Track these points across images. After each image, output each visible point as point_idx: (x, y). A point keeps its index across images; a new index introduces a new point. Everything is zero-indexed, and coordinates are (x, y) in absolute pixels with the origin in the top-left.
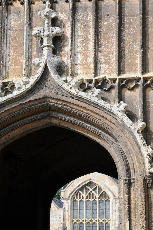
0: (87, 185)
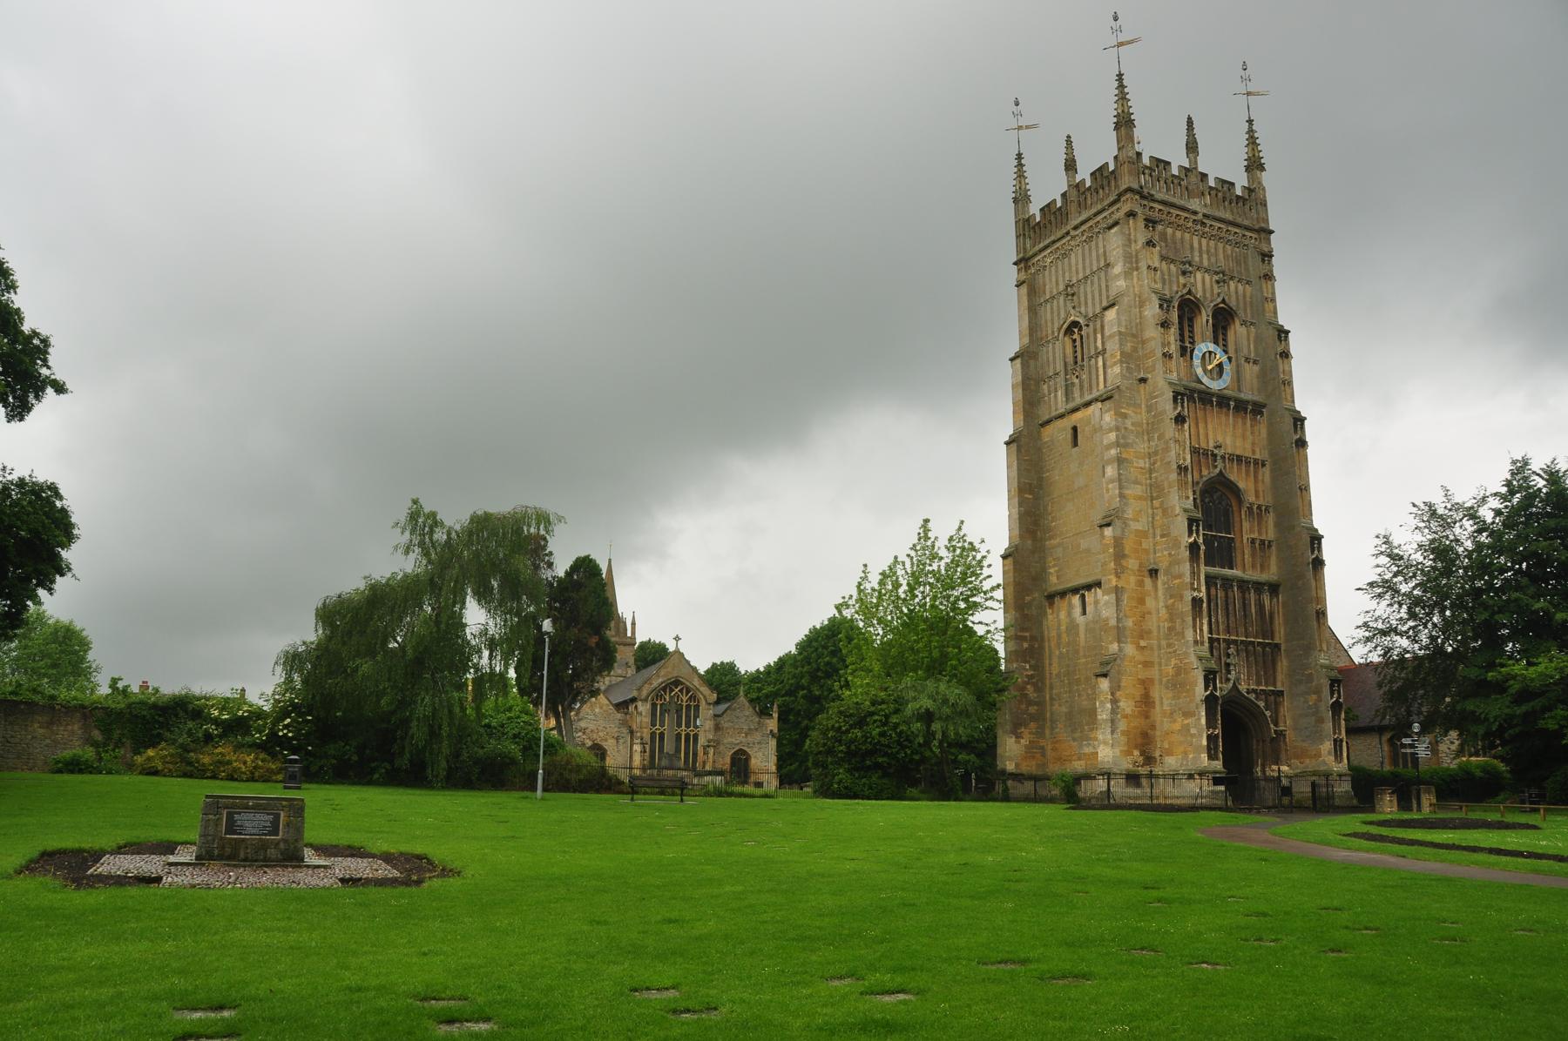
0: (670, 683)
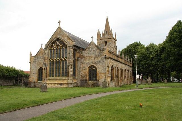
0: (56, 40)
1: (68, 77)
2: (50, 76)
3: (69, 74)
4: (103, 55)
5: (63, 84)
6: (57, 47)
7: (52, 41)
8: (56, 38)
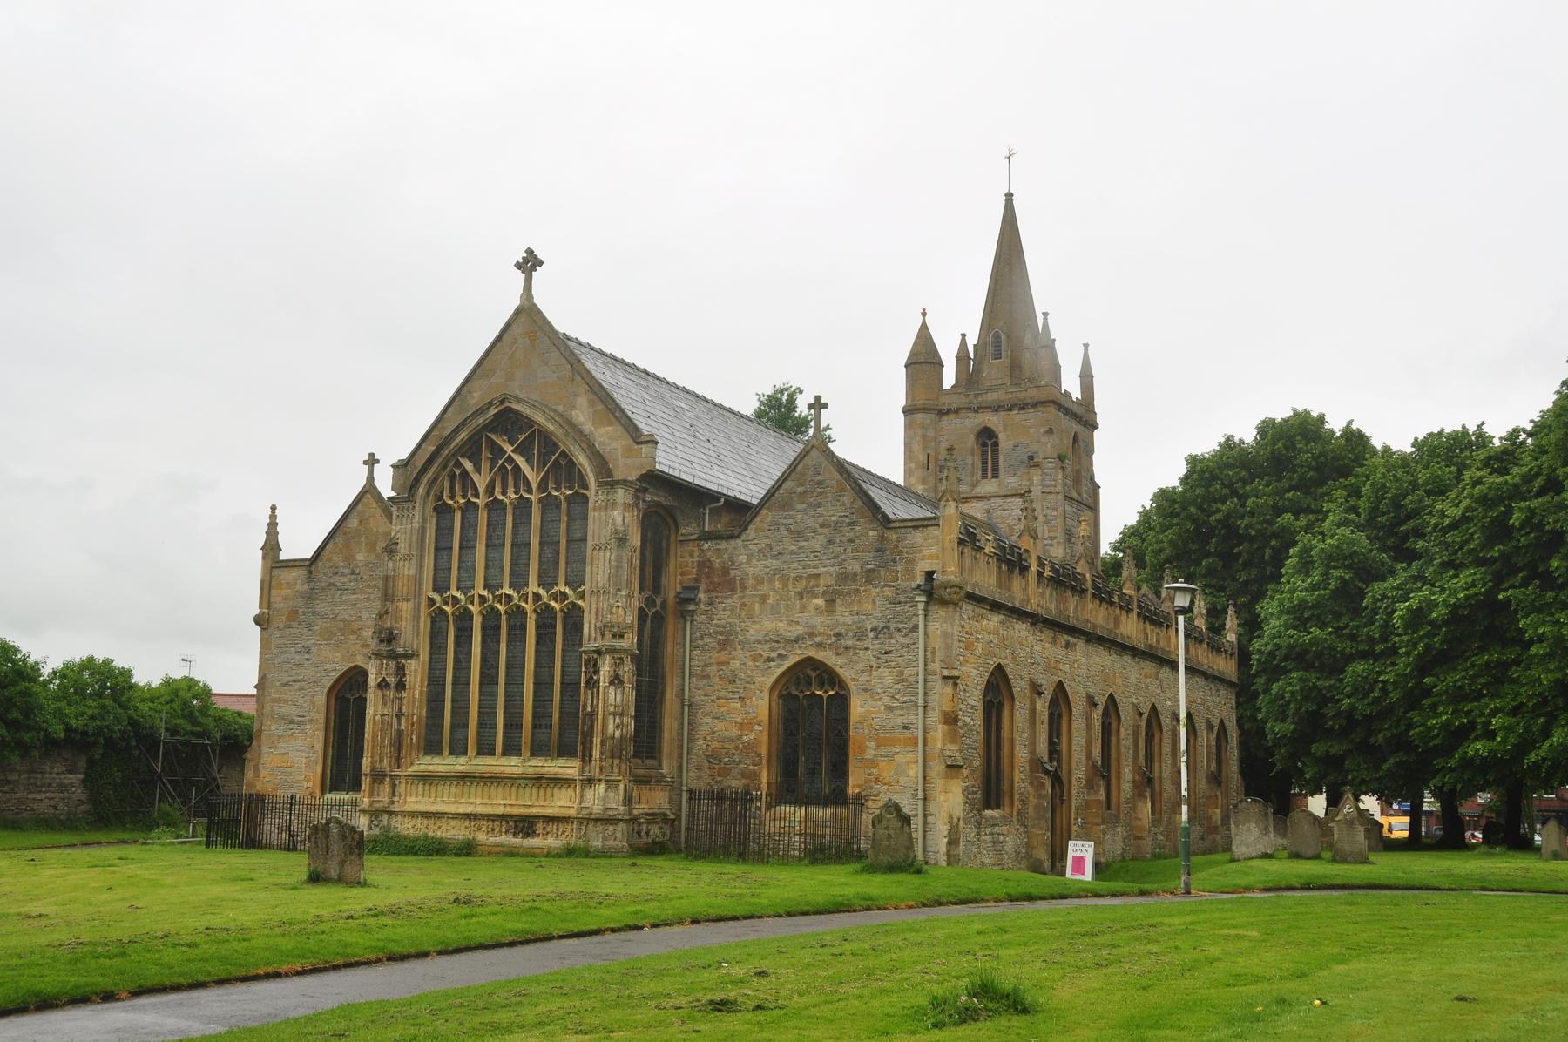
1: (586, 758)
2: (432, 746)
3: (597, 740)
4: (910, 573)
5: (539, 826)
6: (498, 490)
7: (456, 431)
8: (493, 411)
